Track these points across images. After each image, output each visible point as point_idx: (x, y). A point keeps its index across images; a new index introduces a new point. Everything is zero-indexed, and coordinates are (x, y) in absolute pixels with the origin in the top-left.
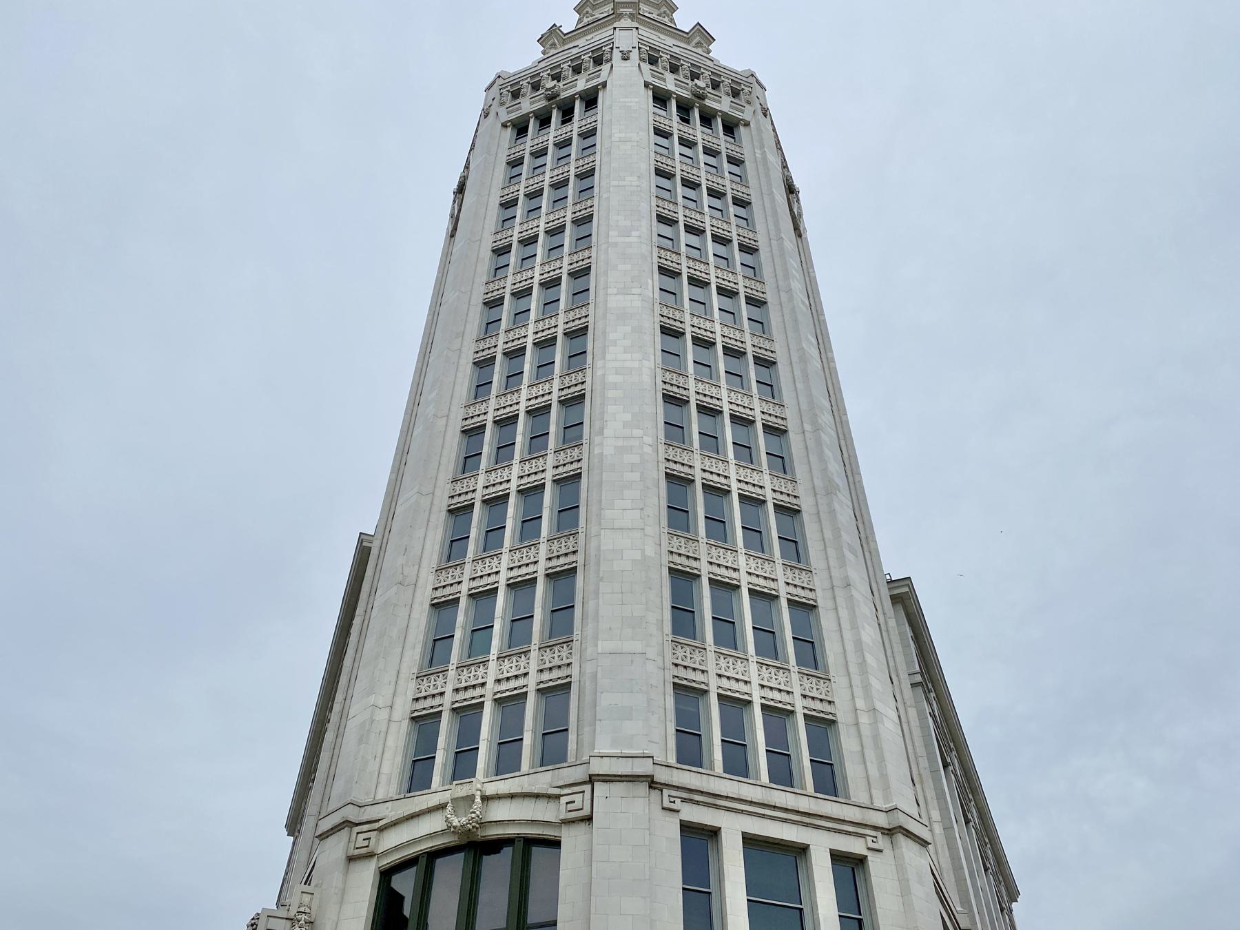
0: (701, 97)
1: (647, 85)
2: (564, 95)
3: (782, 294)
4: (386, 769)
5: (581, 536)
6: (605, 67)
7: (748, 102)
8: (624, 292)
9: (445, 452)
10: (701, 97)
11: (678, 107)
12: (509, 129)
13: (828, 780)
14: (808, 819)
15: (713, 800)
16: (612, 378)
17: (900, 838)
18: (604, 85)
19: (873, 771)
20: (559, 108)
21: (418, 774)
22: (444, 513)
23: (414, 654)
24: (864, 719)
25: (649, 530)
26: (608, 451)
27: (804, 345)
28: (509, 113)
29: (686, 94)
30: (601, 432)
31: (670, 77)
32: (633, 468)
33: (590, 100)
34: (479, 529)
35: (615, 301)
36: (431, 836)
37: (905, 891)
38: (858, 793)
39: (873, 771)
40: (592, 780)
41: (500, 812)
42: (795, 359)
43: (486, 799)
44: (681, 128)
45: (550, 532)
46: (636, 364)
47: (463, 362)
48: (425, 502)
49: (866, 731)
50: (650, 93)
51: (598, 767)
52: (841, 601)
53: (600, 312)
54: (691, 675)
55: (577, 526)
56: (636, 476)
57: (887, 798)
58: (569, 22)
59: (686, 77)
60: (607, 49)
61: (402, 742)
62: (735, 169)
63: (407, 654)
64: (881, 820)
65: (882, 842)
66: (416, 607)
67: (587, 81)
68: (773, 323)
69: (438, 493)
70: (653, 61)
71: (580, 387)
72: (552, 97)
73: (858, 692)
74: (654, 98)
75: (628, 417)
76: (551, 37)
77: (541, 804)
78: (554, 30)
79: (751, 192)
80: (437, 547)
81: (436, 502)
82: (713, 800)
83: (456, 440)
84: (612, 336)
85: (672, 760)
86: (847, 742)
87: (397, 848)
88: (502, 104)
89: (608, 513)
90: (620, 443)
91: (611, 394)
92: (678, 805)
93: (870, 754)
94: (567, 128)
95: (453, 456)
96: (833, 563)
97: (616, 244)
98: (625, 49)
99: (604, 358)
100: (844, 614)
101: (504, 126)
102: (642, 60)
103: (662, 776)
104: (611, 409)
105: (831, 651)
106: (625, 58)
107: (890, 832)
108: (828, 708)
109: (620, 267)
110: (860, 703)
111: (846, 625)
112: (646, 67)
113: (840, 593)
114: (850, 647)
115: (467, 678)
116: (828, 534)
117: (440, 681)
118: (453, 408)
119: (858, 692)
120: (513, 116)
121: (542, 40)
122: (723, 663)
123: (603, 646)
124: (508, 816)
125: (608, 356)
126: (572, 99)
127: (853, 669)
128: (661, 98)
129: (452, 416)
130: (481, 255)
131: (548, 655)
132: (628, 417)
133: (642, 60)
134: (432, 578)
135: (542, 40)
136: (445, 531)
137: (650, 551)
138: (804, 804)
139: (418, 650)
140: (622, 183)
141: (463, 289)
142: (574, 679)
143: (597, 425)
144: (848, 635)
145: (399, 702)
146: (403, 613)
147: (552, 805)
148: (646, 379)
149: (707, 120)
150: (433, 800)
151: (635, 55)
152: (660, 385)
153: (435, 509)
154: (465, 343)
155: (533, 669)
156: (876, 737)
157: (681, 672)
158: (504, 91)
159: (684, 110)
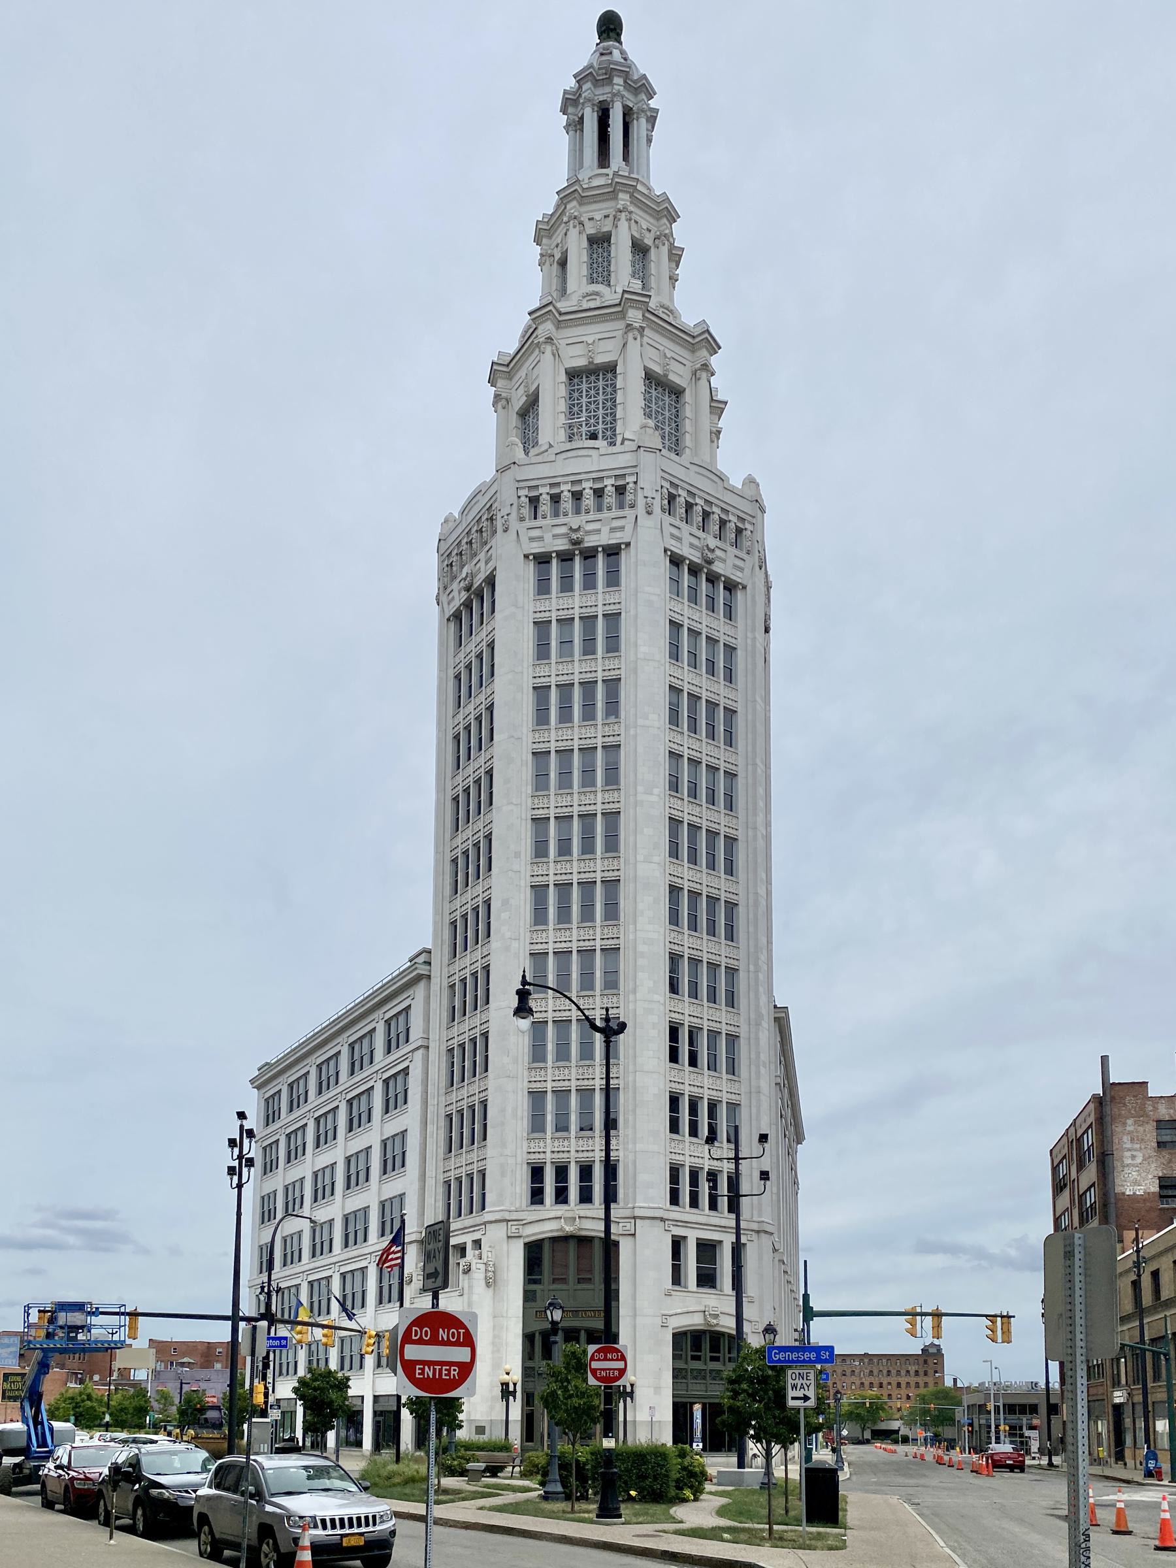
0: (710, 562)
1: (665, 550)
2: (590, 542)
6: (627, 512)
10: (710, 562)
12: (532, 564)
15: (686, 1224)
16: (641, 948)
26: (639, 1011)
28: (532, 539)
30: (635, 991)
31: (683, 525)
35: (644, 870)
37: (760, 1259)
40: (634, 1218)
51: (638, 1213)
57: (760, 1216)
67: (613, 530)
74: (671, 561)
84: (640, 906)
88: (522, 519)
89: (639, 1060)
91: (640, 962)
92: (672, 1228)
99: (635, 923)
101: (526, 556)
103: (666, 1215)
104: (640, 975)
109: (645, 830)
116: (753, 1056)
120: (536, 548)
125: (639, 926)
128: (676, 561)
132: (651, 984)
133: (663, 510)
134: (526, 1073)
137: (662, 1087)
151: (657, 509)
158: (522, 493)
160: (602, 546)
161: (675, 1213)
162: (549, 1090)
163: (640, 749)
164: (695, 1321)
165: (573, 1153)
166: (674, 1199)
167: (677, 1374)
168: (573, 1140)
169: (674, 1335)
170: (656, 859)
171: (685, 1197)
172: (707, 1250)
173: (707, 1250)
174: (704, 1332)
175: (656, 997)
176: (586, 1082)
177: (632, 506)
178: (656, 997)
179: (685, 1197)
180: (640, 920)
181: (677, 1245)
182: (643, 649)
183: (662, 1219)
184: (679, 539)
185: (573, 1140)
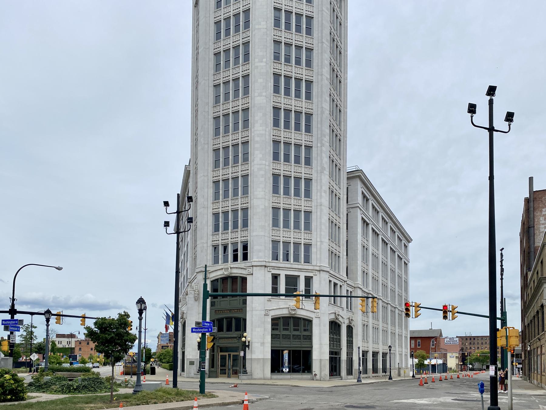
3: (320, 77)
4: (208, 258)
9: (209, 159)
13: (307, 260)
14: (300, 270)
15: (279, 268)
17: (321, 272)
19: (318, 256)
21: (216, 261)
23: (211, 228)
24: (319, 244)
36: (221, 275)
38: (314, 263)
39: (318, 256)
40: (253, 266)
41: (235, 271)
43: (231, 268)
48: (206, 179)
49: (318, 247)
52: (319, 210)
54: (276, 238)
61: (211, 252)
63: (209, 227)
64: (318, 268)
65: (317, 273)
66: (209, 214)
69: (209, 175)
73: (318, 236)
77: (243, 270)
80: (212, 195)
82: (279, 268)
85: (270, 260)
86: (313, 249)
87: (214, 277)
93: (318, 252)
96: (318, 197)
100: (319, 213)
105: (314, 225)
107: (319, 271)
108: (310, 241)
110: (318, 240)
111: (318, 217)
113: (319, 207)
114: (318, 224)
115: (224, 237)
117: (218, 237)
119: (318, 236)
122: (284, 233)
123: (254, 234)
124: (236, 272)
127: (318, 230)
131: (242, 233)
138: (300, 267)
139: (211, 227)
142: (249, 240)
144: (318, 220)
145: (209, 241)
146: (206, 216)
147: (245, 270)
150: (220, 267)
154: (210, 108)
155: (239, 236)
156: (320, 248)
157: (274, 237)
161: (275, 264)
162: (220, 212)
164: (285, 312)
165: (230, 239)
166: (275, 257)
167: (273, 337)
168: (230, 234)
169: (272, 319)
171: (281, 257)
172: (292, 281)
173: (292, 281)
174: (290, 317)
176: (235, 207)
179: (281, 257)
181: (275, 278)
183: (265, 266)
185: (230, 234)
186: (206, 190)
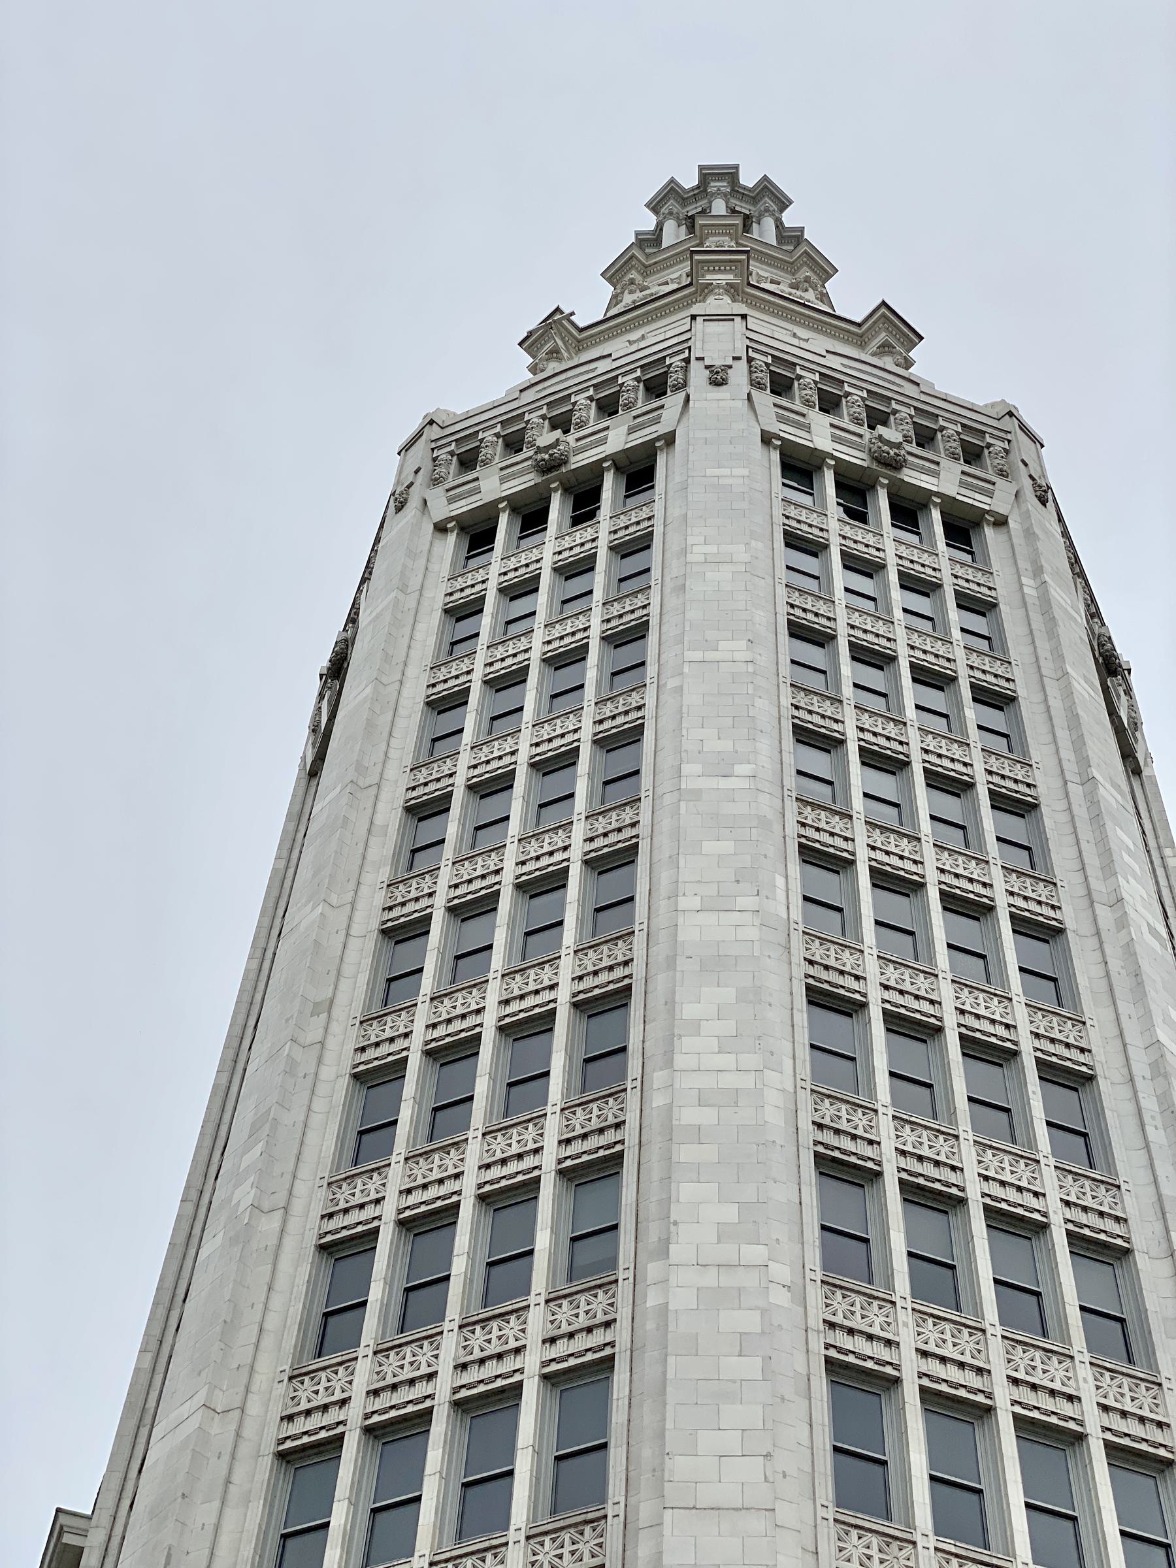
1: (767, 439)
2: (578, 461)
3: (1102, 912)
5: (613, 1527)
7: (1002, 473)
8: (718, 904)
10: (896, 465)
11: (838, 485)
12: (452, 538)
16: (689, 1115)
18: (670, 439)
20: (566, 490)
22: (267, 1461)
25: (786, 1513)
26: (681, 1299)
27: (1162, 1036)
28: (451, 501)
29: (856, 457)
30: (663, 1251)
32: (743, 1345)
33: (638, 472)
34: (353, 1503)
42: (1140, 1067)
44: (848, 531)
45: (534, 1516)
46: (748, 1081)
47: (327, 1073)
48: (221, 1431)
50: (776, 456)
53: (660, 951)
55: (604, 1500)
56: (752, 1367)
58: (590, 303)
59: (857, 421)
60: (676, 361)
62: (995, 719)
67: (631, 431)
68: (1082, 981)
69: (254, 1407)
70: (781, 386)
71: (610, 1137)
72: (550, 466)
75: (731, 1213)
76: (551, 336)
78: (556, 321)
79: (1038, 777)
81: (249, 1432)
83: (305, 1270)
84: (689, 1011)
88: (436, 481)
89: (680, 1466)
90: (710, 1279)
91: (686, 1153)
94: (584, 534)
95: (297, 1309)
97: (697, 794)
98: (718, 362)
99: (669, 1063)
102: (757, 384)
104: (686, 1191)
106: (718, 379)
112: (765, 400)
118: (301, 1188)
120: (462, 507)
121: (529, 343)
125: (680, 1061)
126: (595, 471)
128: (799, 467)
129: (297, 1206)
130: (379, 820)
132: (731, 1213)
133: (757, 384)
135: (529, 343)
136: (270, 1504)
140: (711, 656)
141: (334, 899)
143: (653, 1233)
148: (775, 1118)
149: (908, 512)
151: (739, 375)
152: (809, 1134)
153: (244, 1450)
159: (855, 492)
160: (612, 457)
163: (692, 698)
170: (749, 902)
175: (754, 1253)
177: (678, 388)
178: (754, 1253)
180: (688, 1043)
182: (699, 551)
184: (807, 428)
186: (205, 1513)
